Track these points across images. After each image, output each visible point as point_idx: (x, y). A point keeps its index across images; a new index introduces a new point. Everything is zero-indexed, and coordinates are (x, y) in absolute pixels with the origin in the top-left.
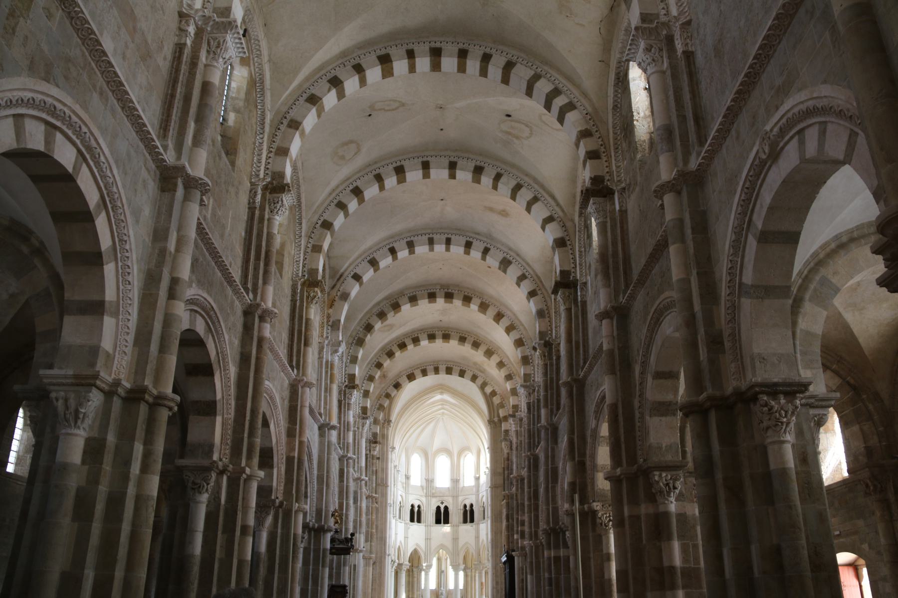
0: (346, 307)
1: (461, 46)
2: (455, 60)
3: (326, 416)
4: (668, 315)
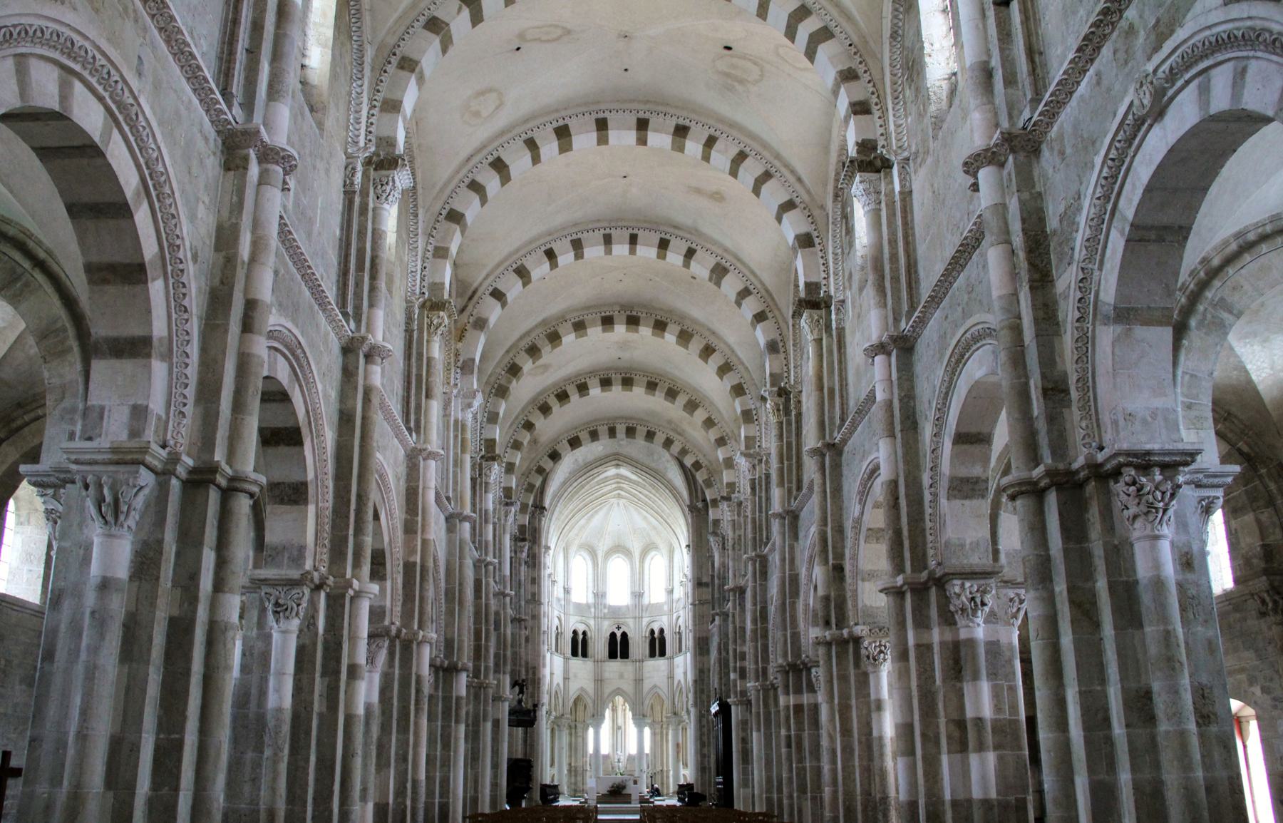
0: (482, 340)
3: (456, 502)
4: (978, 349)
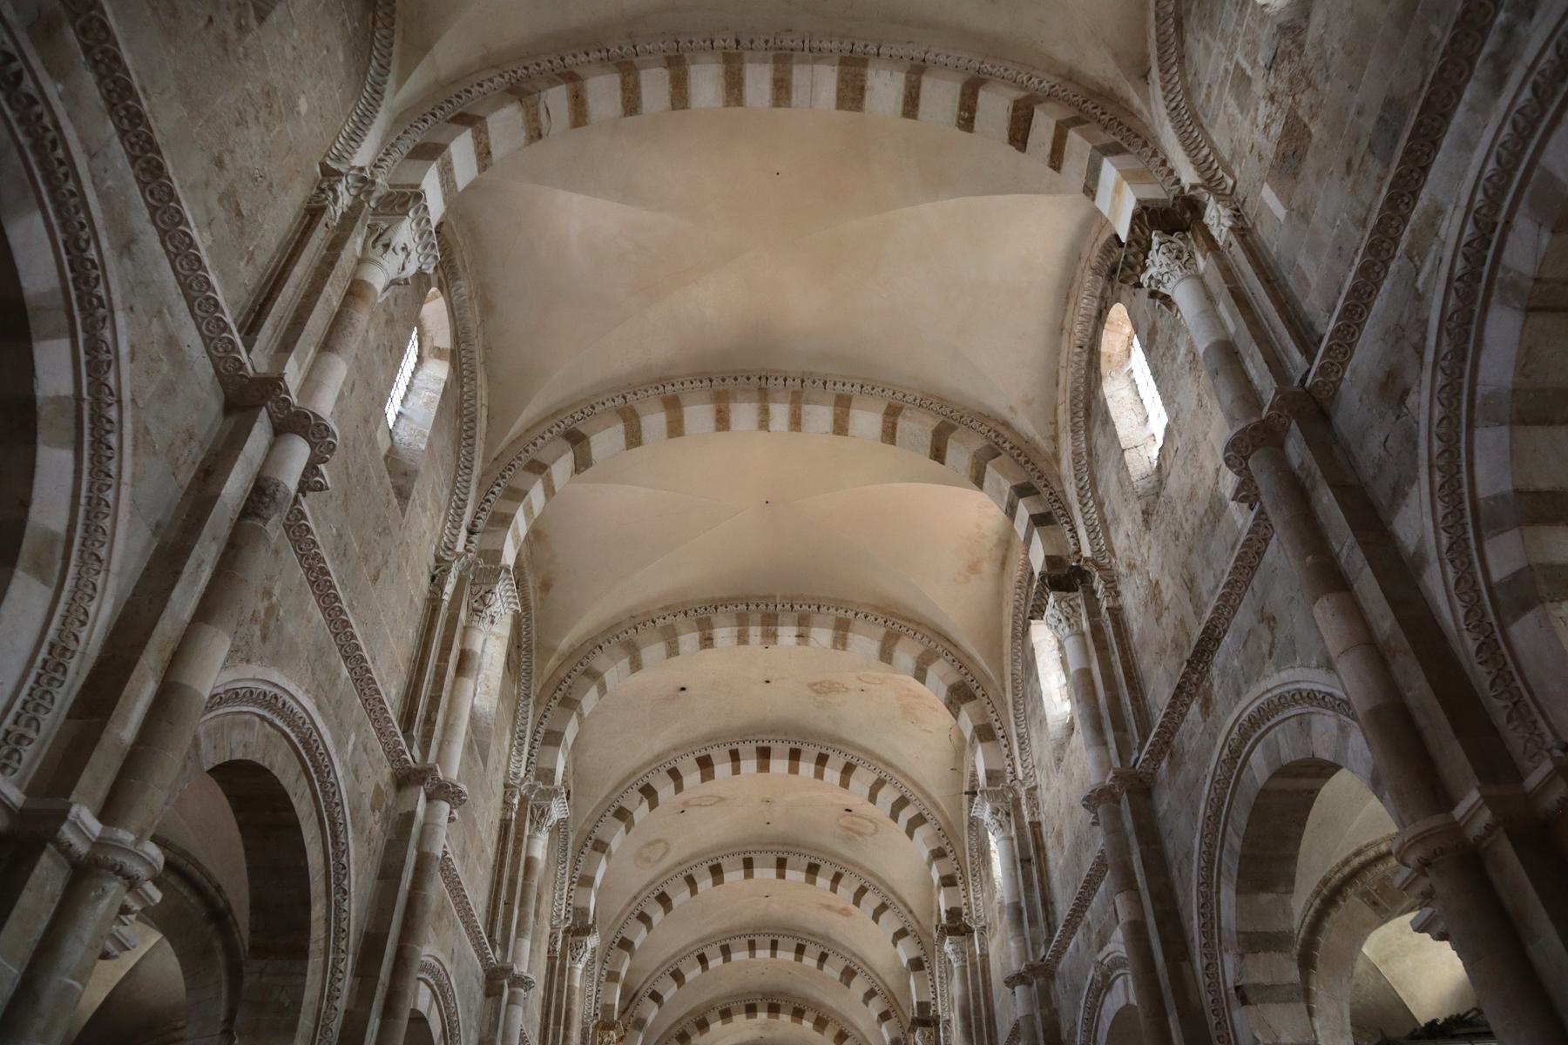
0: (641, 1039)
1: (793, 745)
2: (786, 762)
